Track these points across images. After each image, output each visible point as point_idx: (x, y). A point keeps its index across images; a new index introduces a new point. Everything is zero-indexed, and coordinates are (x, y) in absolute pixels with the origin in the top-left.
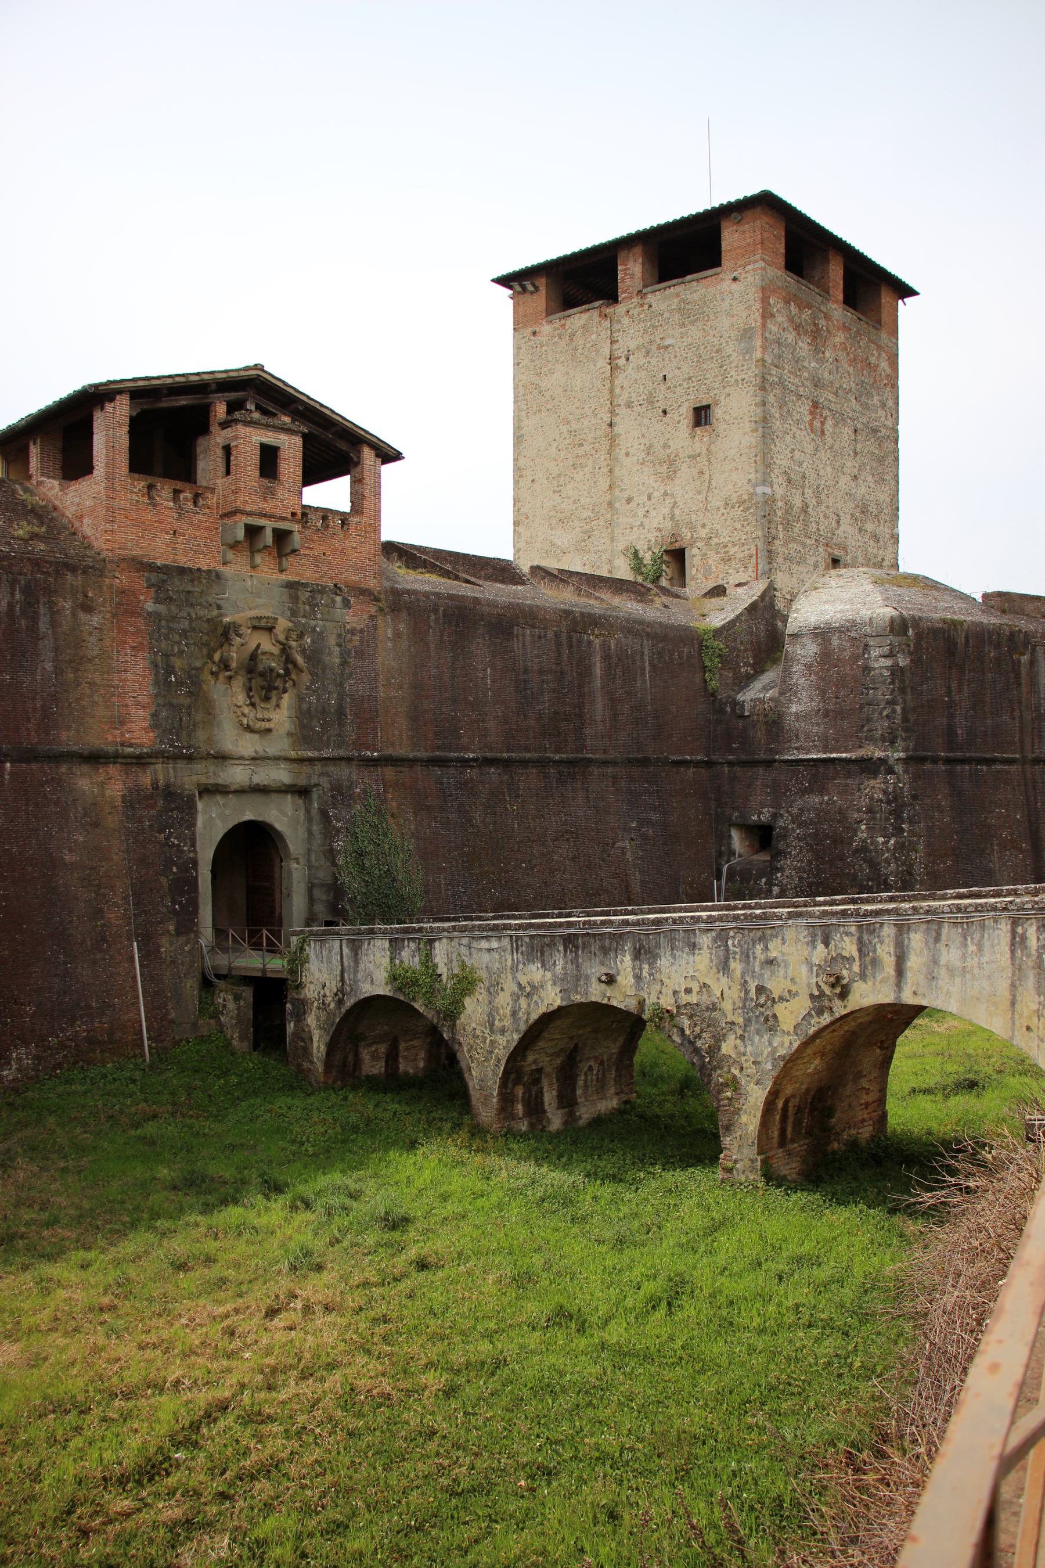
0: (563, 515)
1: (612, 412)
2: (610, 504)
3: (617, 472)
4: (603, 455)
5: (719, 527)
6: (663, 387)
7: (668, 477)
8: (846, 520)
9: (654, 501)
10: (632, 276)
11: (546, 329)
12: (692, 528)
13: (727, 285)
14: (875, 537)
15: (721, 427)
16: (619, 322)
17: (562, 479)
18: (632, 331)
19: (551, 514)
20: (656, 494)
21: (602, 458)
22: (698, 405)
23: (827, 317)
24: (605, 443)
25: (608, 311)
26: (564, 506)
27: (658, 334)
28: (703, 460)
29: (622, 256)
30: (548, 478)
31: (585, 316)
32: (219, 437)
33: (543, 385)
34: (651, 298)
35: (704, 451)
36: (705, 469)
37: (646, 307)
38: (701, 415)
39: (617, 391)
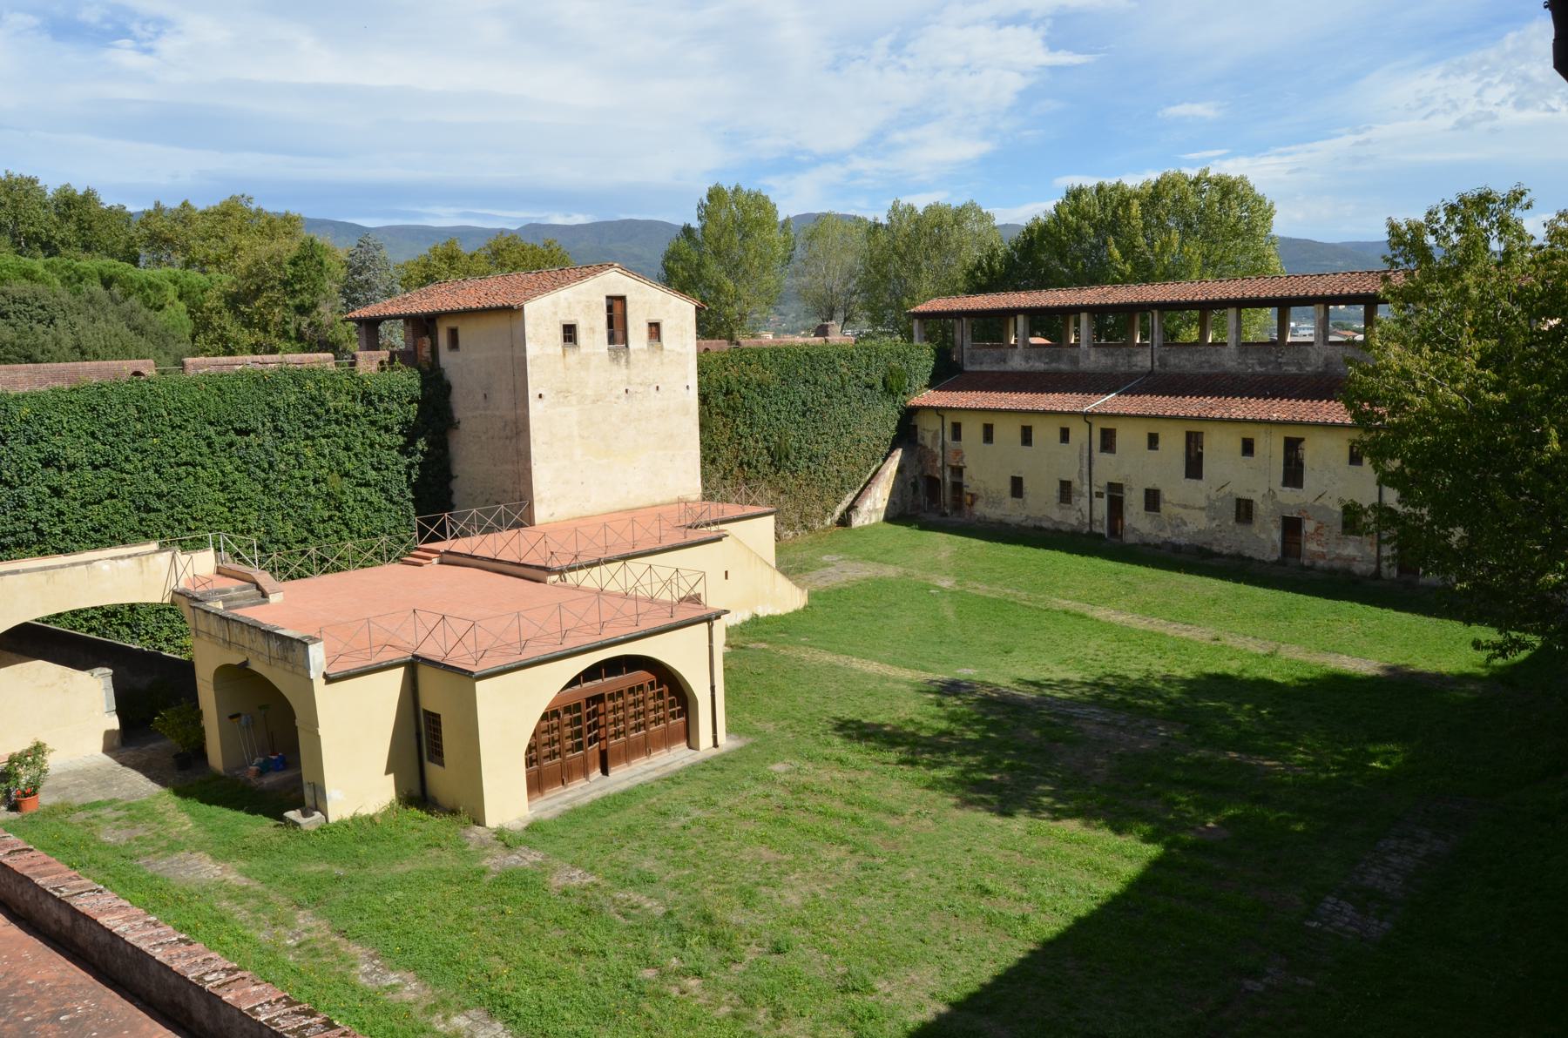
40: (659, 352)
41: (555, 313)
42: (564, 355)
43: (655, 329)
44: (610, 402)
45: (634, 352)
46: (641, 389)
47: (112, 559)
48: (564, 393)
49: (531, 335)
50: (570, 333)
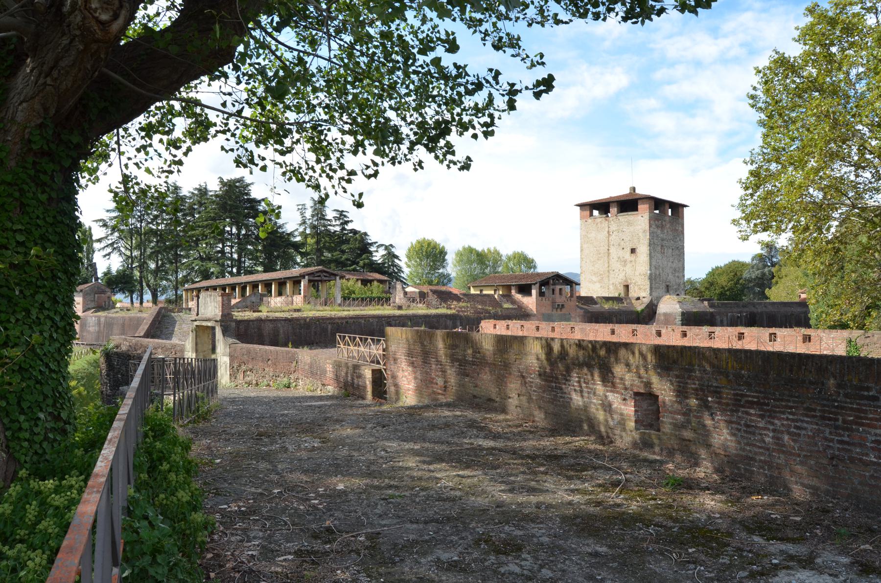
2: (608, 271)
4: (606, 258)
6: (623, 242)
8: (670, 274)
13: (640, 217)
14: (678, 277)
15: (638, 255)
23: (665, 221)
28: (634, 264)
29: (611, 204)
32: (552, 287)
33: (589, 236)
34: (619, 217)
38: (633, 251)
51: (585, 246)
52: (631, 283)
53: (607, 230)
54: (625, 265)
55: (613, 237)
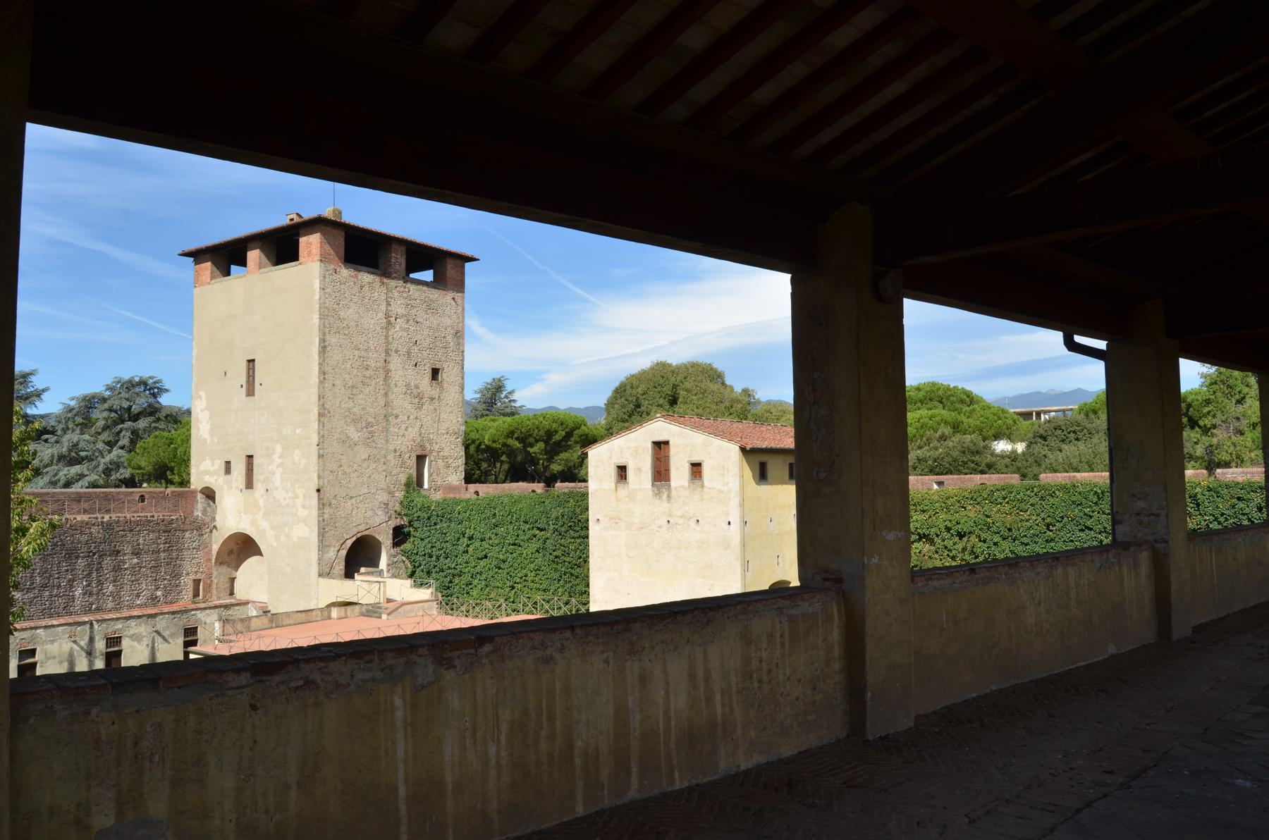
0: (355, 417)
1: (387, 353)
3: (391, 397)
5: (444, 446)
7: (419, 408)
9: (410, 421)
10: (400, 265)
11: (345, 272)
12: (431, 444)
16: (391, 291)
17: (355, 390)
18: (399, 302)
19: (346, 414)
20: (412, 417)
21: (381, 383)
22: (434, 367)
24: (382, 371)
25: (385, 280)
26: (355, 410)
27: (414, 311)
29: (394, 246)
30: (345, 386)
31: (372, 277)
35: (437, 397)
36: (438, 408)
37: (407, 290)
38: (435, 373)
39: (390, 339)
40: (699, 489)
41: (611, 457)
42: (616, 490)
43: (696, 467)
44: (653, 530)
45: (676, 489)
46: (681, 522)
47: (362, 581)
48: (615, 520)
49: (592, 475)
50: (622, 471)
51: (332, 340)
52: (431, 451)
53: (383, 307)
54: (420, 408)
55: (397, 331)
